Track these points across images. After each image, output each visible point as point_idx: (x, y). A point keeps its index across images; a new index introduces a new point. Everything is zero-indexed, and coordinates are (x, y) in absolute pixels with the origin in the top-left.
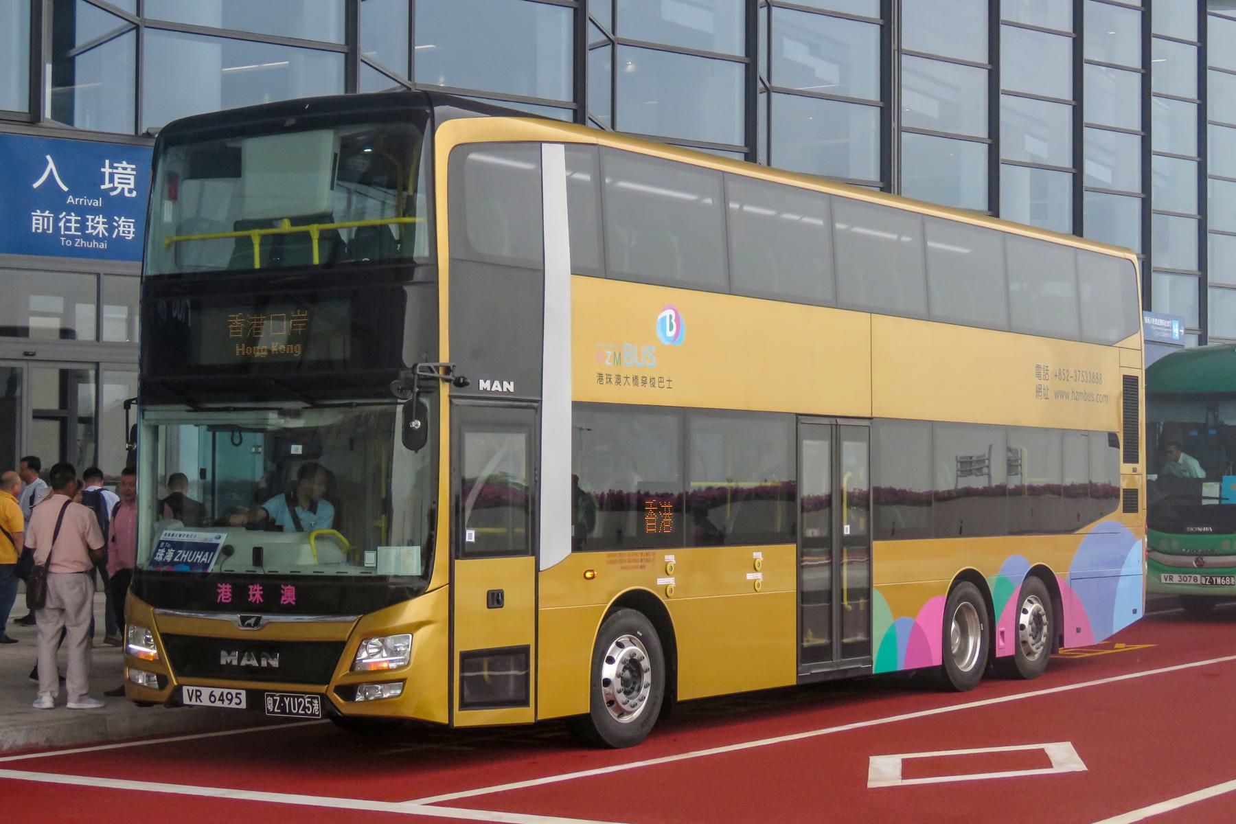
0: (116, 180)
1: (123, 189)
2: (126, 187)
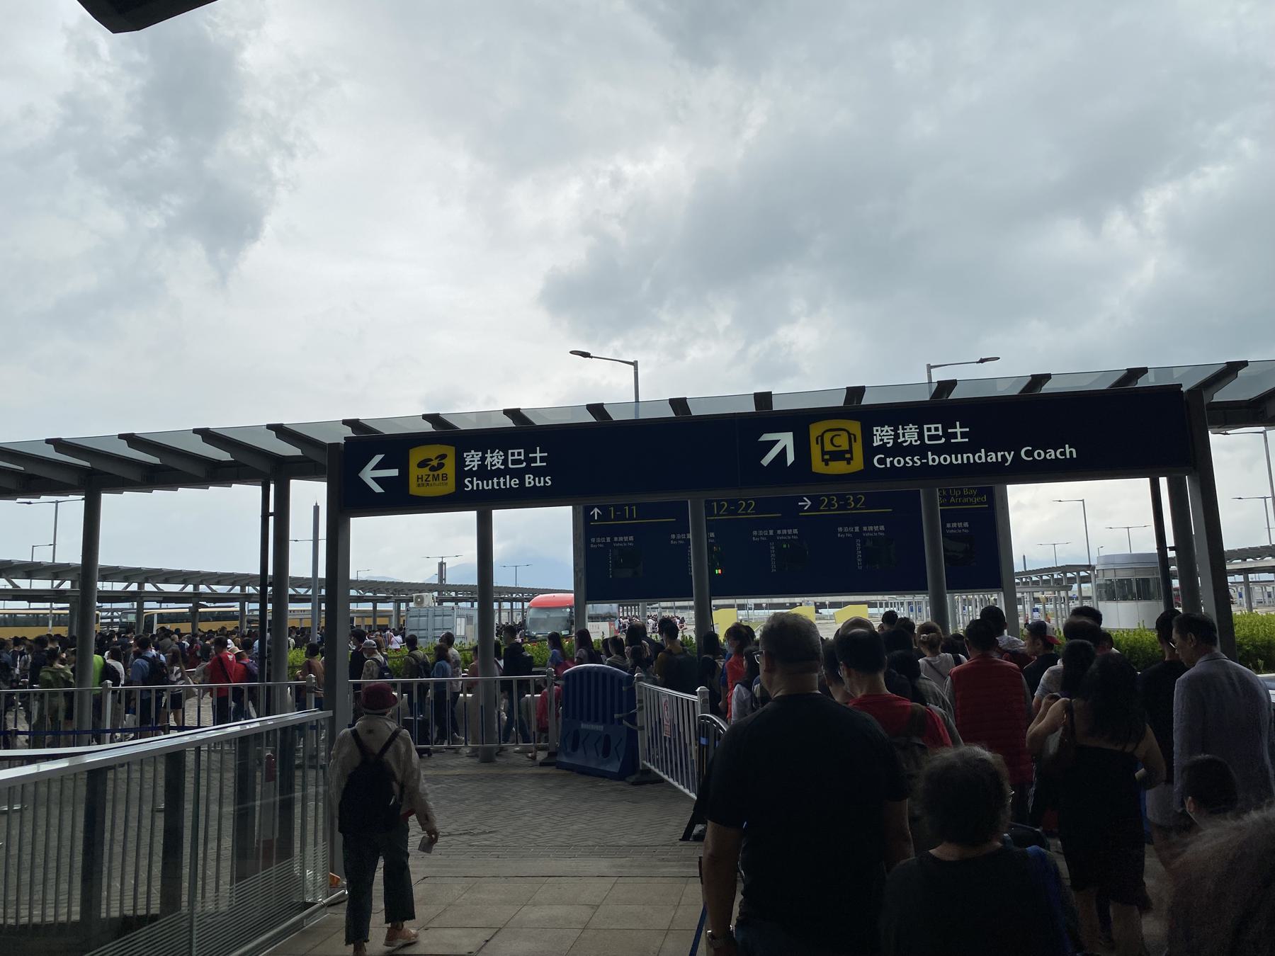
0: (906, 437)
1: (911, 441)
2: (913, 440)
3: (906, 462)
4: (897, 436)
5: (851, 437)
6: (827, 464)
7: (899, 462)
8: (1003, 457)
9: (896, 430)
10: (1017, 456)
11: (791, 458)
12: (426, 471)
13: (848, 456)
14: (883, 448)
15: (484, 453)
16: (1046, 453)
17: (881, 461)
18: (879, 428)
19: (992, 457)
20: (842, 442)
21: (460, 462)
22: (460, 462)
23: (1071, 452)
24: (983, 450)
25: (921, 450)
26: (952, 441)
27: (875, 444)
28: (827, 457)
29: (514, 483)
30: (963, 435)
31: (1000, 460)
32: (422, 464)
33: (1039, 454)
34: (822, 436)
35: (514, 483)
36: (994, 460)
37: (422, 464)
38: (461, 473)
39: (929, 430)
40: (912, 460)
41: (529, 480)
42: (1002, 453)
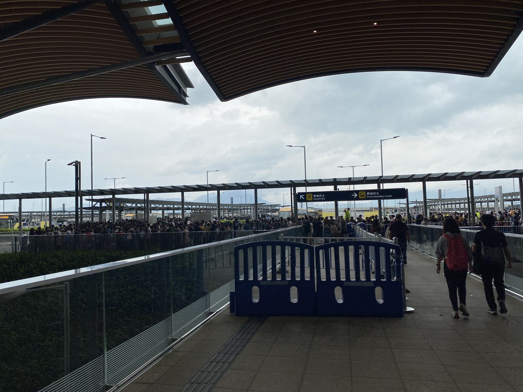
4: (370, 194)
5: (364, 194)
10: (385, 196)
12: (308, 197)
17: (368, 197)
21: (313, 196)
22: (313, 196)
25: (373, 195)
29: (320, 199)
32: (308, 196)
33: (387, 196)
35: (320, 199)
37: (308, 196)
38: (313, 197)
41: (322, 199)
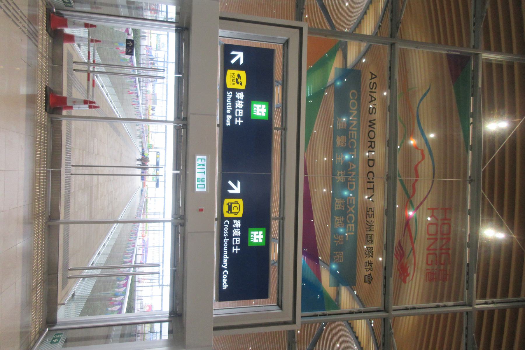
2: (235, 234)
3: (226, 231)
4: (236, 228)
6: (227, 204)
7: (226, 229)
8: (224, 265)
9: (239, 228)
10: (225, 269)
11: (230, 191)
13: (230, 212)
14: (232, 223)
15: (243, 101)
16: (225, 279)
18: (240, 222)
19: (225, 261)
20: (235, 210)
23: (225, 287)
24: (228, 258)
25: (230, 236)
26: (233, 247)
27: (234, 221)
28: (230, 204)
30: (235, 251)
31: (224, 263)
33: (225, 277)
34: (238, 203)
36: (224, 261)
39: (238, 239)
40: (226, 234)
42: (226, 264)
